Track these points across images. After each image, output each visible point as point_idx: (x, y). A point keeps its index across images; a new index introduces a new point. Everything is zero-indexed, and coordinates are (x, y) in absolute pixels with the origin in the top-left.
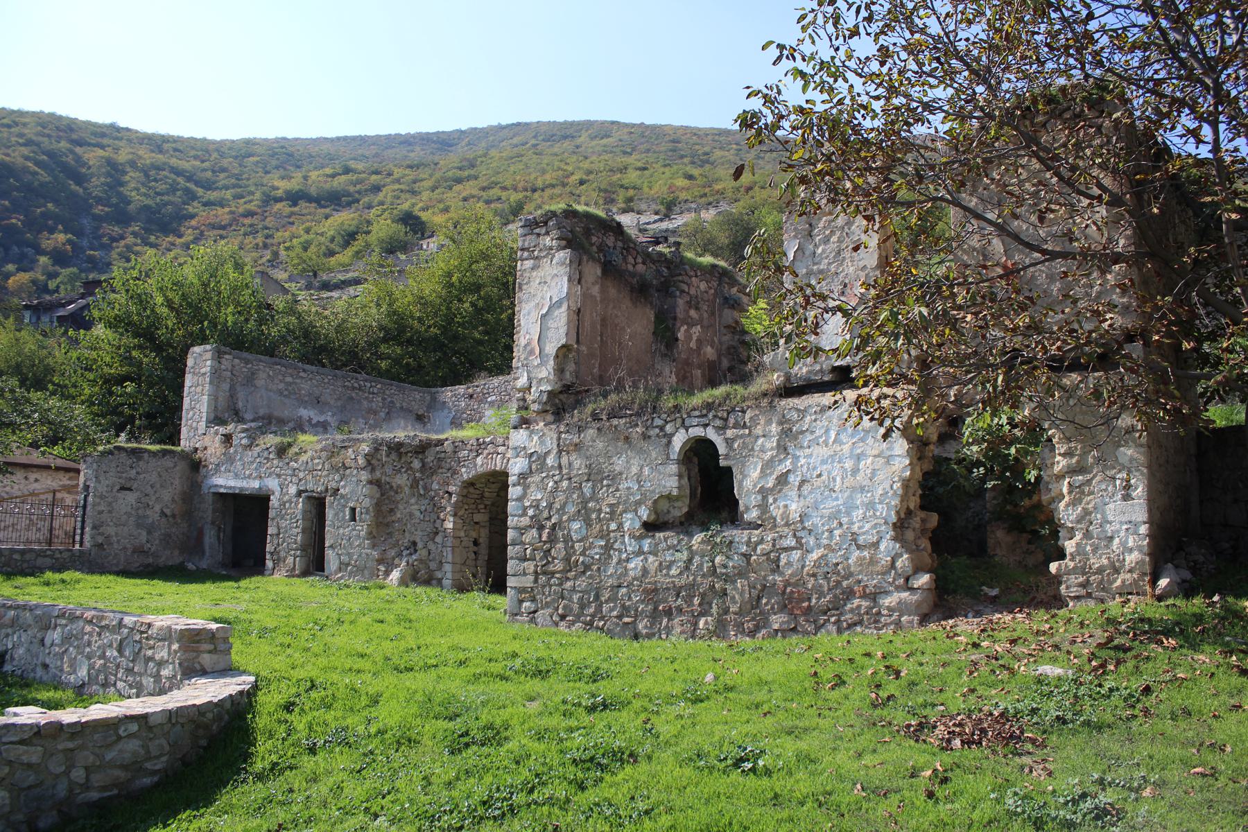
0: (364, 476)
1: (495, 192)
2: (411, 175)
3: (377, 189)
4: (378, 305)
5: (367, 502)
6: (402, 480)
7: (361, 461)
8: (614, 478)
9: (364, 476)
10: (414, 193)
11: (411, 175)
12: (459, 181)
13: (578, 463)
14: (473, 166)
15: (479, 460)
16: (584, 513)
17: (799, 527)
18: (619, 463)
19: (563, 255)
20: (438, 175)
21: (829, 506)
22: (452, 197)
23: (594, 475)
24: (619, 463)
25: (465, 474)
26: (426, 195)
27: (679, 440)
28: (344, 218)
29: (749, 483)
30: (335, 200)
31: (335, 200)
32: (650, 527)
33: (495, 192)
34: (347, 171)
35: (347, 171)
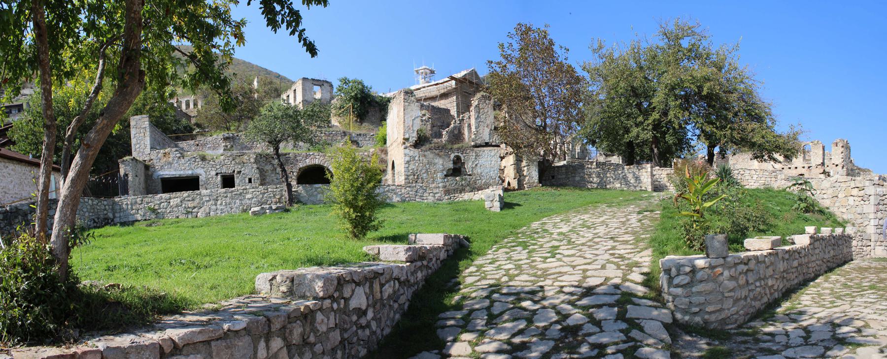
0: (255, 166)
5: (258, 175)
6: (268, 167)
7: (252, 160)
8: (435, 164)
9: (255, 166)
13: (425, 161)
15: (307, 161)
16: (427, 172)
17: (481, 175)
18: (436, 161)
21: (486, 171)
23: (429, 163)
24: (436, 161)
25: (301, 165)
27: (452, 156)
29: (468, 166)
32: (446, 176)
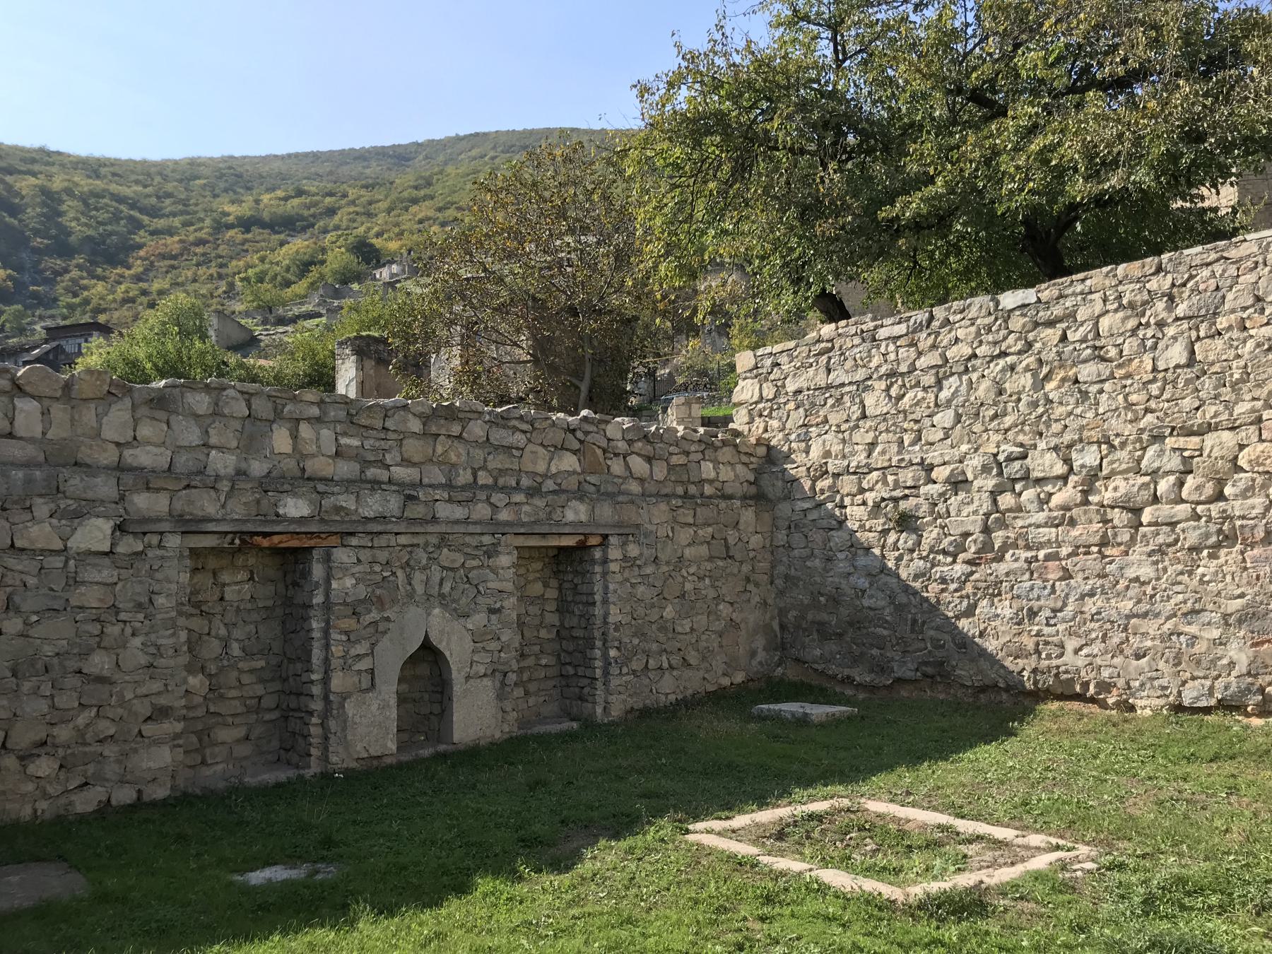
1: (451, 213)
2: (366, 195)
3: (331, 212)
4: (304, 359)
10: (369, 215)
11: (366, 195)
12: (415, 201)
14: (429, 184)
19: (353, 358)
20: (394, 196)
22: (407, 220)
26: (381, 219)
28: (299, 245)
30: (288, 225)
31: (288, 225)
33: (451, 213)
34: (300, 193)
35: (300, 193)
